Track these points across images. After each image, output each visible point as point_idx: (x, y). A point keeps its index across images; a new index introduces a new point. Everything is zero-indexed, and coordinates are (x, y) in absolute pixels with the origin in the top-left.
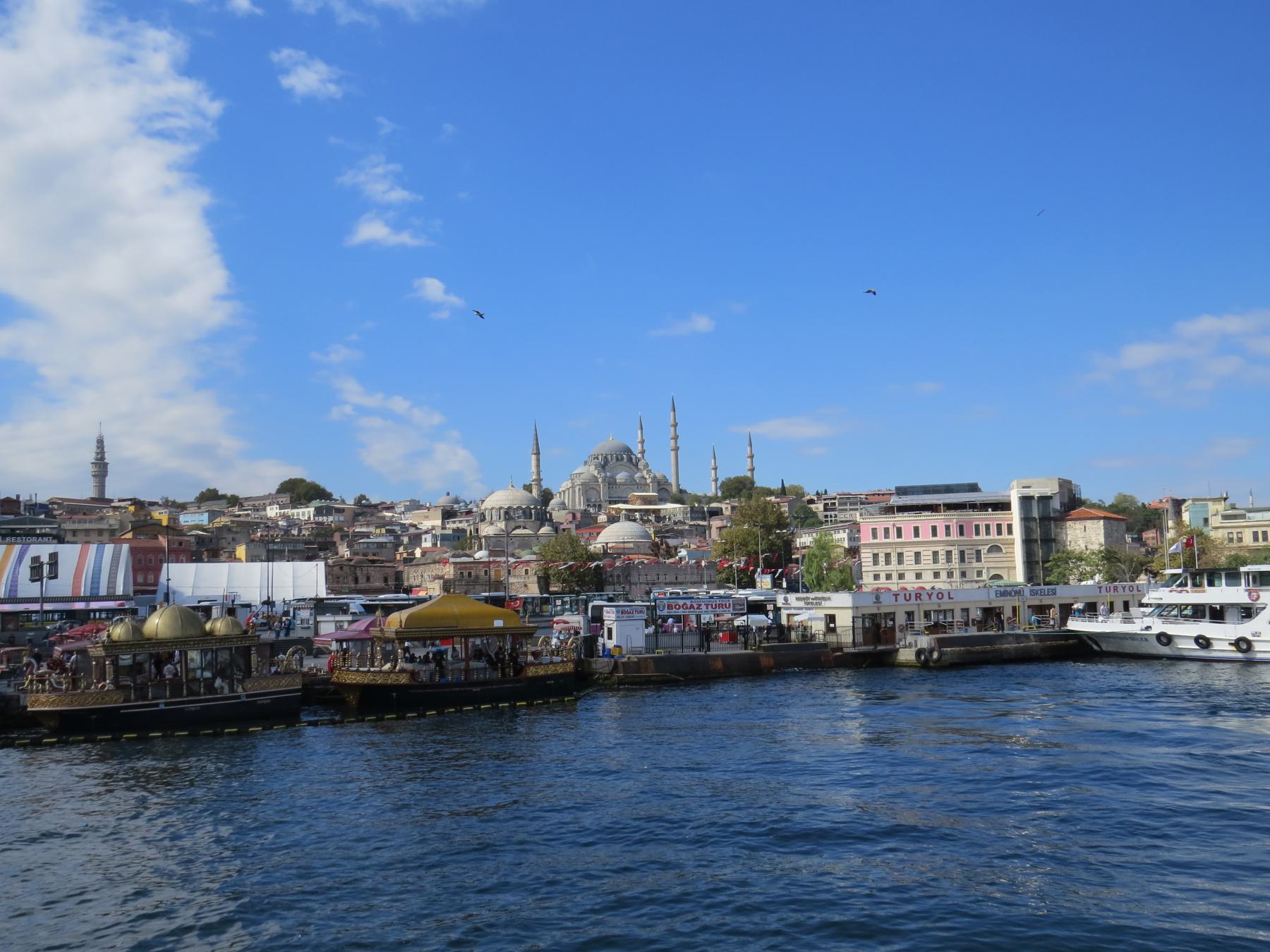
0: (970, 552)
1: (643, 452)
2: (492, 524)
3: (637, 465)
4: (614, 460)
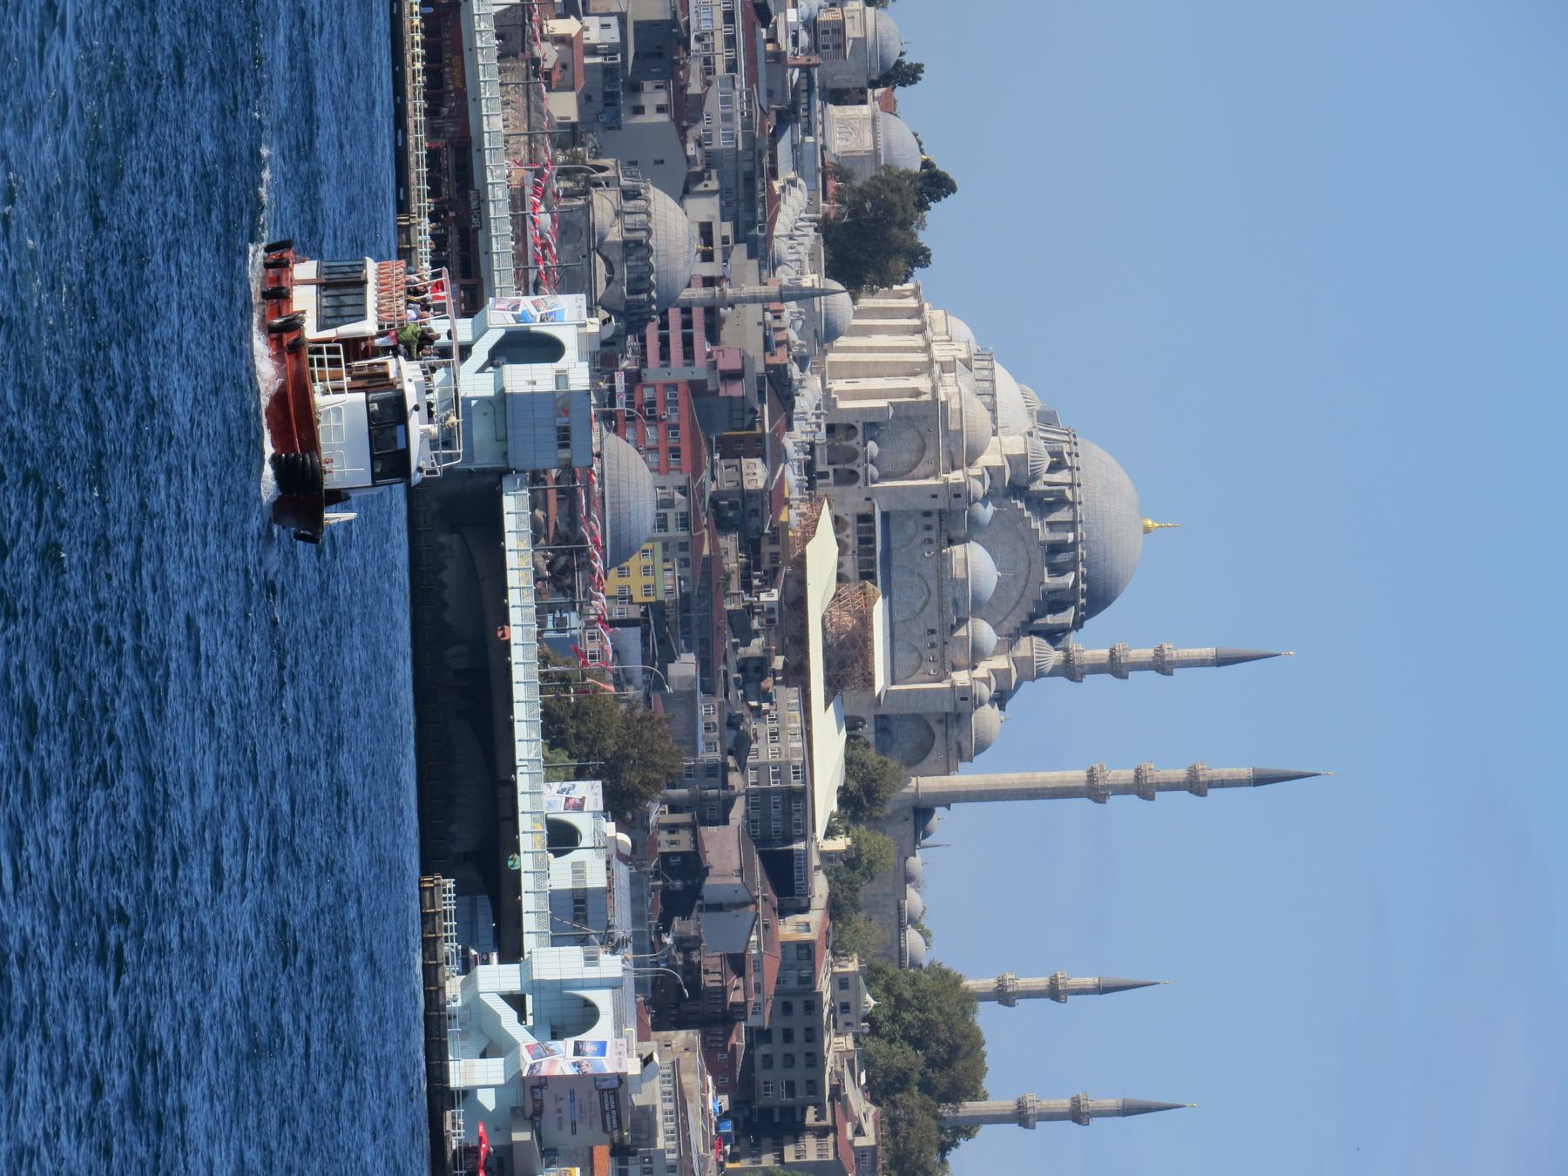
2: (619, 214)
3: (1028, 628)
4: (1046, 535)
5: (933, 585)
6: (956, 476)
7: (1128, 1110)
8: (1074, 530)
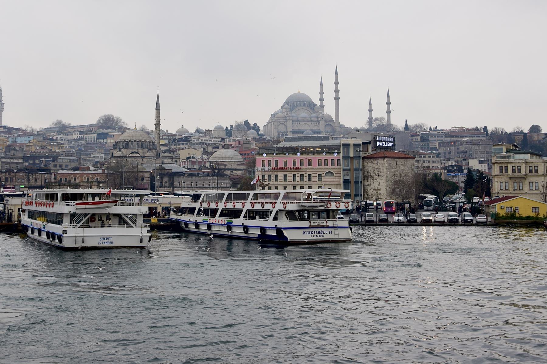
0: (315, 175)
1: (322, 100)
5: (305, 123)
7: (388, 96)
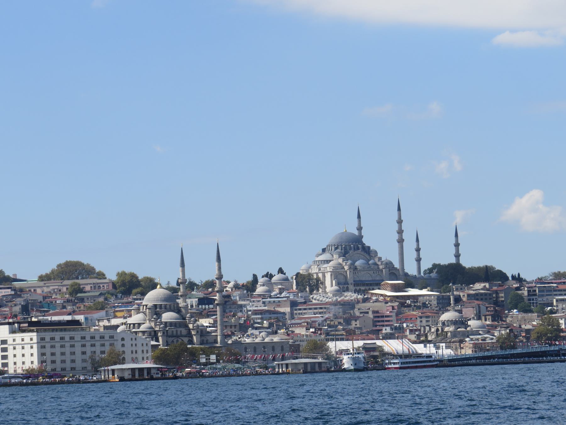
2: (448, 326)
5: (365, 272)
6: (346, 268)
8: (350, 245)
